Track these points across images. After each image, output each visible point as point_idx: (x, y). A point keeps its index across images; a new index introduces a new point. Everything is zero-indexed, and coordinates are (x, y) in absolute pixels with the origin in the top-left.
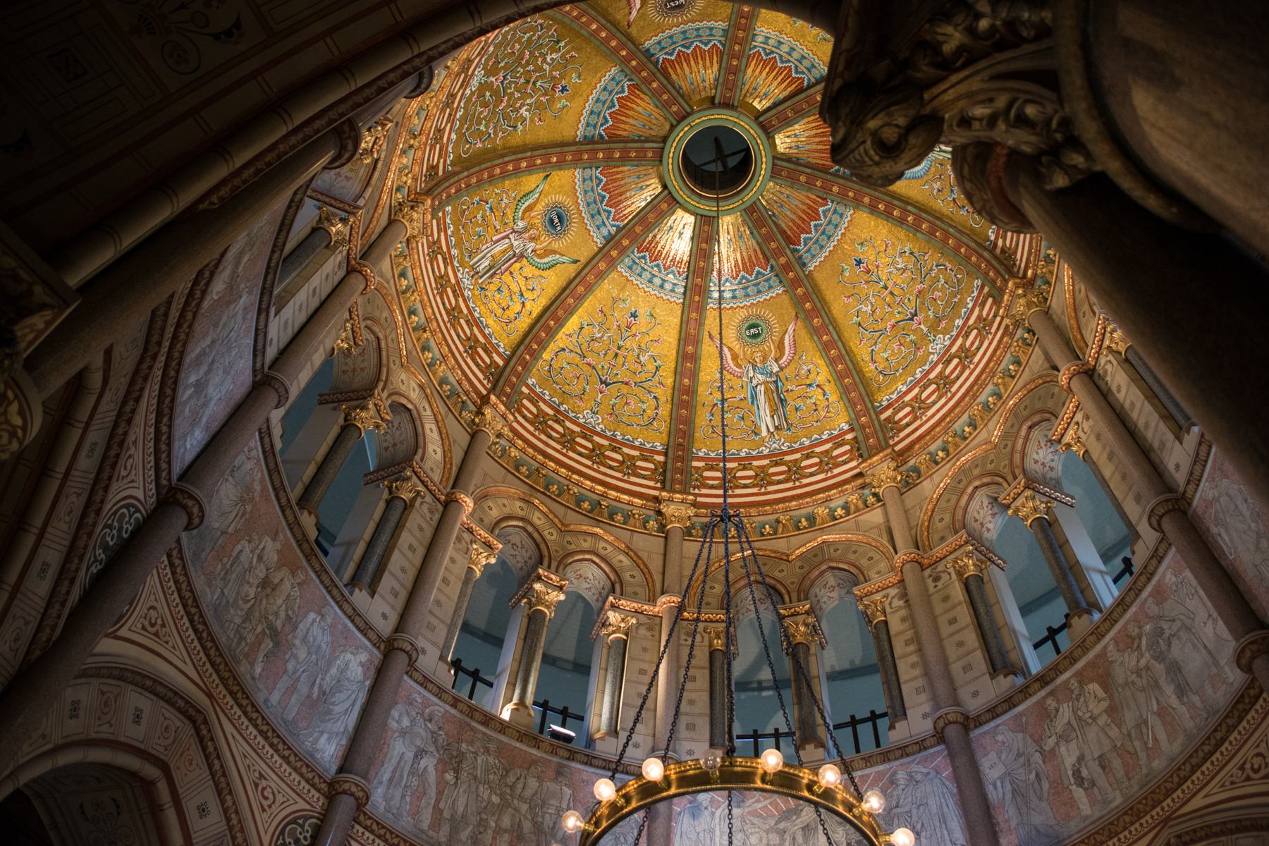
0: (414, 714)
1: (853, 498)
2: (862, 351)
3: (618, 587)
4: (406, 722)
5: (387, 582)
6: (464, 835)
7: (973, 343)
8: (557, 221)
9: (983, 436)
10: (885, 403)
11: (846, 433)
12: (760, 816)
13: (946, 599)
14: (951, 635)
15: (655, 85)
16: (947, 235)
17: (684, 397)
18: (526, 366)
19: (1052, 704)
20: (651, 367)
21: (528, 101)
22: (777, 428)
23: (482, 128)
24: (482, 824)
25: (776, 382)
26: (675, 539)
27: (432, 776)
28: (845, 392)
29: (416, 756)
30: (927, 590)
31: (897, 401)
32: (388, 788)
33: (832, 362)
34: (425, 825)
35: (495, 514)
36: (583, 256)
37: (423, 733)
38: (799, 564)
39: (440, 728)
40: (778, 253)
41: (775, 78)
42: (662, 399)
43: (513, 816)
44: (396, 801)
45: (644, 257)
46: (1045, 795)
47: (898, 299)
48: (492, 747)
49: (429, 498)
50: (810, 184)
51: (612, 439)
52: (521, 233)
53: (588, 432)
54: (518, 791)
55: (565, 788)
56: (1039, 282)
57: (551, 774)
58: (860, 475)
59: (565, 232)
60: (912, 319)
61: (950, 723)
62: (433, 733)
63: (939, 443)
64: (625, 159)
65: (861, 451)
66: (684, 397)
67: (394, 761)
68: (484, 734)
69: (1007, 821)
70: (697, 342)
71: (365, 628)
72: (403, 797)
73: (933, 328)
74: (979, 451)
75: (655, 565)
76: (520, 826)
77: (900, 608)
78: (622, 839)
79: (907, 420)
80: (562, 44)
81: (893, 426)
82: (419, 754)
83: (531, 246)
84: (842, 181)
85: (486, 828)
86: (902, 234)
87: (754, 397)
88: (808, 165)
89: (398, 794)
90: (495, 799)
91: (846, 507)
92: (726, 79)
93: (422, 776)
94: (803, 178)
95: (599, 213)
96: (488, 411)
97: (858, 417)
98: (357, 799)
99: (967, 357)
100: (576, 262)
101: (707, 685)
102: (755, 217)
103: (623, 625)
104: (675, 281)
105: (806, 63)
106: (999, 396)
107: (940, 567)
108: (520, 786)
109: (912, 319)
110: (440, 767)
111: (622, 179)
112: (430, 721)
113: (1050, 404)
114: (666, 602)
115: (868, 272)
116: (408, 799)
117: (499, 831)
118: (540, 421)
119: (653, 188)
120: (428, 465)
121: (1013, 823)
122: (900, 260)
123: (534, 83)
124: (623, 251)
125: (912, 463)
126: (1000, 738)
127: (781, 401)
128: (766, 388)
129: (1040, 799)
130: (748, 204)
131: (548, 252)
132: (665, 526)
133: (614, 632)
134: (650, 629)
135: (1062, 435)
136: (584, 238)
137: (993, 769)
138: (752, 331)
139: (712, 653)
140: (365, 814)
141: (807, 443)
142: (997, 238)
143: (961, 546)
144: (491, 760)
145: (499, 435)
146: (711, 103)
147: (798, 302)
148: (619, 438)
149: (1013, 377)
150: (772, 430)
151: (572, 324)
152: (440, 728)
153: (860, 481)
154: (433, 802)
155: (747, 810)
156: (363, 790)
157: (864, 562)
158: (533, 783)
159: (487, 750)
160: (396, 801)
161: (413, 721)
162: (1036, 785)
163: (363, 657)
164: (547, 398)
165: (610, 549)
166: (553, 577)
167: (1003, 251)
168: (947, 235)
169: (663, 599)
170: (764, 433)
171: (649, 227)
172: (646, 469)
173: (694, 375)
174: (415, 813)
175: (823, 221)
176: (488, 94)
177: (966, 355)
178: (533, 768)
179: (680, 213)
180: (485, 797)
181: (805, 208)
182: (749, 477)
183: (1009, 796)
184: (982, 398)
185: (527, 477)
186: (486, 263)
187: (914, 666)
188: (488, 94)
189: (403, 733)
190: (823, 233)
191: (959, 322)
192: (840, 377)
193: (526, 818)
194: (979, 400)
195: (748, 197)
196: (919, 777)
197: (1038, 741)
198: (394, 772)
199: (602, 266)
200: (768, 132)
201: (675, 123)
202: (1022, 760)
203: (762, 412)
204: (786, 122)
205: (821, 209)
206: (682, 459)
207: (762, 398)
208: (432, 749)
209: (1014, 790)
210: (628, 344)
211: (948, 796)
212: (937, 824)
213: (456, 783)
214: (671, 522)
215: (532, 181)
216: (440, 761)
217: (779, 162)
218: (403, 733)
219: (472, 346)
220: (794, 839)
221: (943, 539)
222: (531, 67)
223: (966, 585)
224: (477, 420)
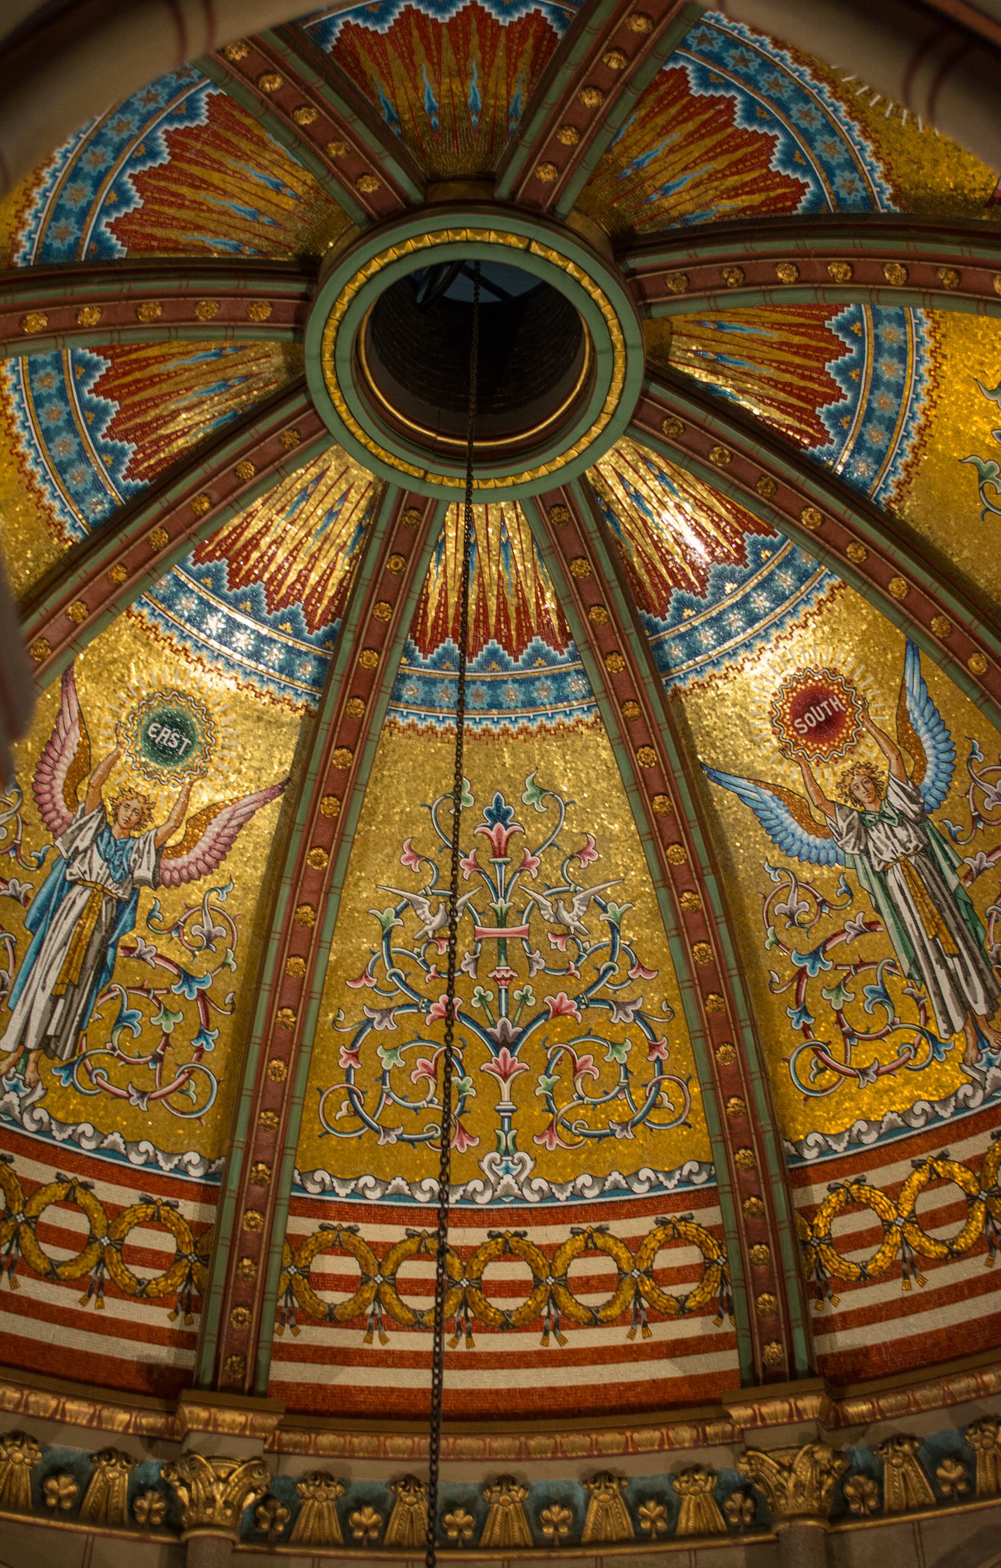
11: (183, 1189)
22: (45, 1042)
41: (783, 366)
45: (91, 367)
47: (504, 971)
60: (497, 1046)
87: (48, 911)
95: (98, 182)
109: (497, 1046)
111: (241, 156)
115: (499, 852)
122: (579, 909)
128: (88, 908)
138: (167, 733)
150: (31, 1042)
190: (494, 685)
203: (39, 971)
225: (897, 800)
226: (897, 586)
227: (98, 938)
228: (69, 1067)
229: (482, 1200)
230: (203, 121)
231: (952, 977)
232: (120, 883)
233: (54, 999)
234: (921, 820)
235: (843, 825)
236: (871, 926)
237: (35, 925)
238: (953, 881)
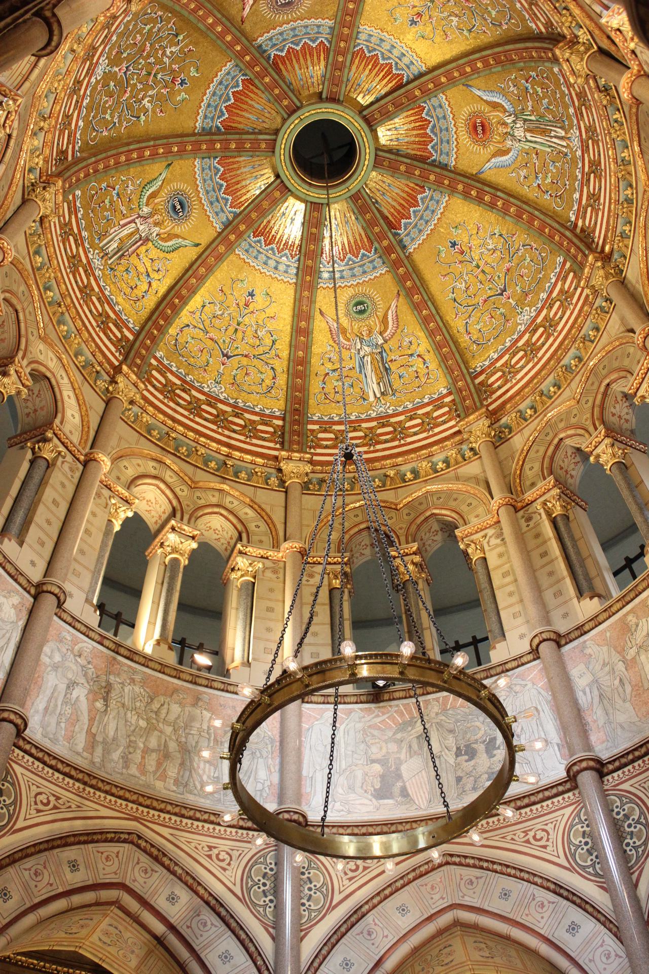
0: (64, 650)
1: (452, 453)
2: (457, 324)
3: (244, 536)
4: (57, 658)
5: (33, 533)
6: (116, 755)
7: (556, 314)
8: (179, 207)
9: (567, 393)
10: (479, 369)
12: (379, 729)
13: (538, 536)
14: (543, 566)
15: (267, 80)
16: (532, 217)
17: (299, 367)
18: (153, 339)
19: (631, 619)
20: (268, 341)
21: (150, 93)
22: (383, 394)
23: (108, 117)
24: (131, 745)
25: (381, 353)
26: (295, 493)
27: (84, 705)
28: (444, 359)
29: (68, 687)
30: (521, 529)
31: (489, 367)
32: (44, 716)
33: (431, 334)
34: (80, 747)
35: (131, 473)
36: (204, 242)
37: (74, 667)
38: (405, 511)
39: (89, 663)
40: (381, 237)
41: (377, 75)
42: (279, 370)
43: (160, 737)
44: (52, 728)
45: (259, 241)
46: (628, 697)
47: (489, 277)
48: (137, 678)
49: (69, 458)
50: (409, 173)
51: (235, 406)
52: (145, 218)
53: (212, 400)
54: (163, 715)
55: (205, 712)
56: (616, 256)
57: (189, 700)
58: (459, 432)
59: (187, 218)
60: (501, 294)
61: (544, 640)
62: (83, 667)
63: (528, 402)
64: (240, 149)
65: (460, 411)
66: (299, 367)
67: (49, 692)
68: (130, 667)
69: (595, 721)
70: (309, 318)
71: (16, 575)
72: (58, 723)
73: (521, 303)
74: (563, 408)
75: (278, 517)
76: (166, 745)
77: (497, 546)
78: (258, 753)
79: (499, 383)
80: (181, 37)
81: (484, 390)
82: (72, 685)
83: (156, 230)
84: (438, 170)
85: (135, 748)
86: (492, 216)
87: (362, 366)
88: (407, 156)
89: (53, 721)
90: (143, 723)
91: (446, 461)
92: (333, 76)
93: (75, 704)
94: (403, 168)
95: (218, 201)
96: (120, 379)
97: (455, 381)
98: (16, 725)
99: (551, 326)
100: (197, 245)
101: (328, 619)
102: (361, 204)
103: (250, 569)
104: (289, 263)
105: (406, 60)
106: (580, 359)
107: (531, 509)
108: (164, 712)
109: (501, 294)
110: (91, 696)
111: (239, 168)
112: (80, 656)
113: (626, 363)
114: (288, 548)
115: (462, 252)
116: (63, 725)
117: (146, 751)
118: (168, 391)
119: (267, 177)
120: (67, 428)
121: (601, 723)
122: (490, 242)
123: (155, 76)
124: (240, 235)
125: (503, 421)
126: (588, 651)
127: (386, 369)
128: (372, 358)
129: (624, 701)
130: (353, 192)
131: (171, 236)
132: (285, 482)
133: (242, 576)
134: (275, 572)
135: (638, 389)
136: (202, 226)
137: (580, 676)
138: (359, 307)
139: (331, 591)
140: (24, 739)
141: (410, 406)
142: (577, 219)
143: (549, 490)
144: (137, 689)
145: (132, 402)
146: (320, 97)
147: (401, 280)
148: (241, 405)
149: (592, 342)
150: (378, 395)
151: (195, 302)
152: (89, 663)
153: (458, 438)
154: (86, 727)
155: (368, 724)
156: (21, 717)
157: (464, 508)
158: (176, 709)
159: (133, 681)
160: (52, 728)
161: (63, 656)
162: (620, 689)
163: (16, 600)
164: (174, 369)
165: (236, 503)
166: (186, 528)
167: (582, 230)
168: (532, 217)
169: (286, 545)
170: (372, 398)
171: (263, 213)
172: (266, 432)
173: (307, 347)
174: (70, 738)
175: (421, 207)
176: (112, 84)
177: (550, 324)
178: (175, 696)
179: (291, 200)
180: (133, 722)
181: (405, 195)
182: (359, 438)
183: (596, 700)
184: (565, 362)
185: (159, 440)
186: (114, 245)
187: (511, 594)
188: (112, 84)
189: (56, 667)
190: (421, 218)
191: (543, 295)
192: (438, 347)
193: (171, 739)
194: (562, 363)
195: (354, 185)
196: (517, 688)
197: (621, 652)
198: (49, 701)
199: (222, 249)
200: (371, 124)
201: (286, 116)
202: (607, 669)
204: (387, 116)
205: (419, 197)
206: (298, 422)
207: (369, 367)
208: (83, 680)
209: (601, 695)
210: (246, 320)
211: (543, 702)
212: (535, 727)
213: (106, 710)
214: (291, 478)
215: (156, 169)
216: (90, 691)
217: (380, 153)
218: (56, 667)
219: (103, 321)
220: (410, 747)
221: (533, 485)
222: (152, 60)
223: (554, 522)
224: (111, 388)
225: (509, 120)
226: (443, 80)
227: (380, 364)
228: (394, 394)
229: (523, 329)
230: (222, 169)
231: (556, 137)
232: (376, 348)
233: (379, 384)
234: (516, 116)
235: (510, 143)
236: (537, 154)
237: (361, 372)
238: (533, 118)
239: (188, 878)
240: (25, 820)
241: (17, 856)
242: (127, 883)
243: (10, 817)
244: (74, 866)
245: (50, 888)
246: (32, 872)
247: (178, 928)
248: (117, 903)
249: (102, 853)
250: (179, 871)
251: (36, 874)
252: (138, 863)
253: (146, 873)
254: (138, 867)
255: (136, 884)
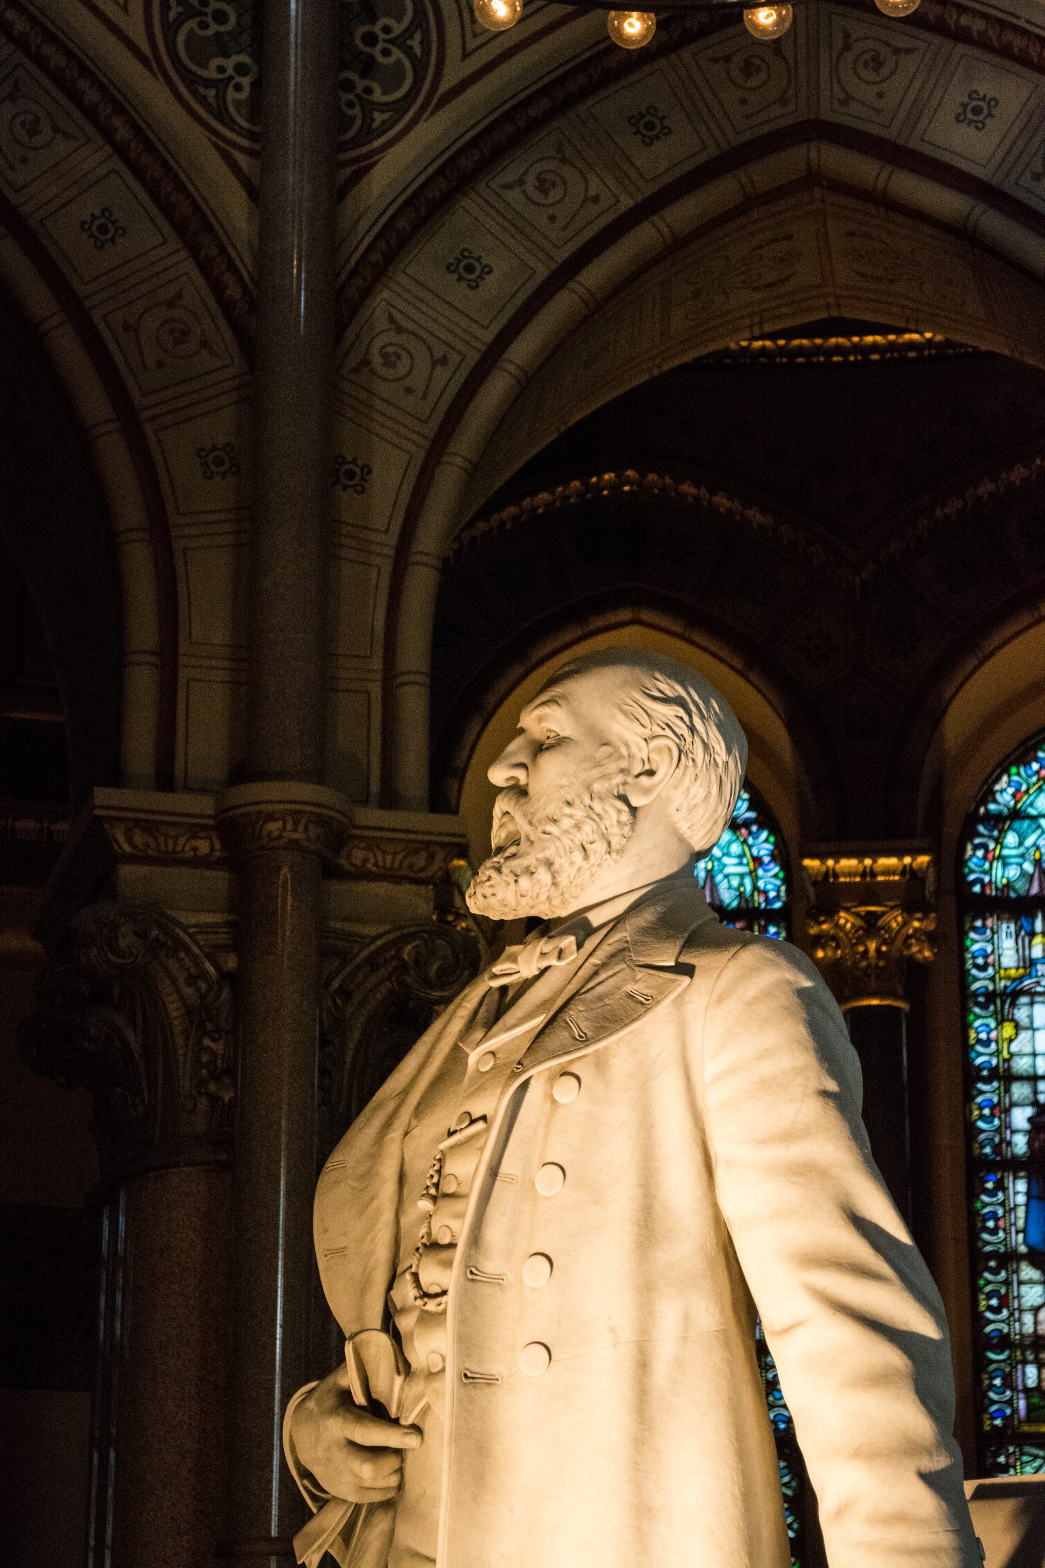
239: (1008, 36)
240: (465, 55)
241: (466, 163)
242: (826, 114)
243: (420, 66)
244: (648, 126)
245: (595, 209)
246: (529, 187)
247: (1009, 188)
248: (813, 178)
249: (728, 59)
250: (978, 25)
251: (543, 186)
252: (847, 47)
253: (877, 63)
254: (849, 57)
255: (854, 108)
